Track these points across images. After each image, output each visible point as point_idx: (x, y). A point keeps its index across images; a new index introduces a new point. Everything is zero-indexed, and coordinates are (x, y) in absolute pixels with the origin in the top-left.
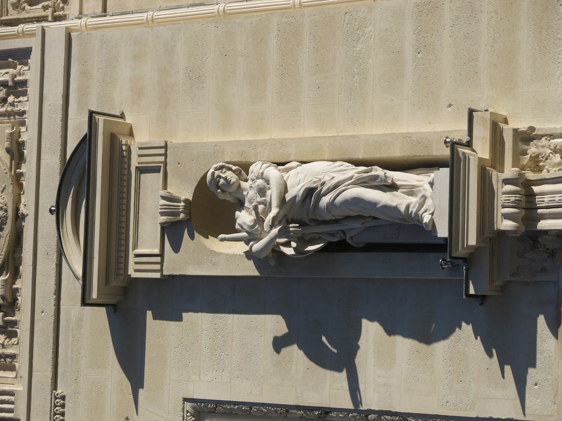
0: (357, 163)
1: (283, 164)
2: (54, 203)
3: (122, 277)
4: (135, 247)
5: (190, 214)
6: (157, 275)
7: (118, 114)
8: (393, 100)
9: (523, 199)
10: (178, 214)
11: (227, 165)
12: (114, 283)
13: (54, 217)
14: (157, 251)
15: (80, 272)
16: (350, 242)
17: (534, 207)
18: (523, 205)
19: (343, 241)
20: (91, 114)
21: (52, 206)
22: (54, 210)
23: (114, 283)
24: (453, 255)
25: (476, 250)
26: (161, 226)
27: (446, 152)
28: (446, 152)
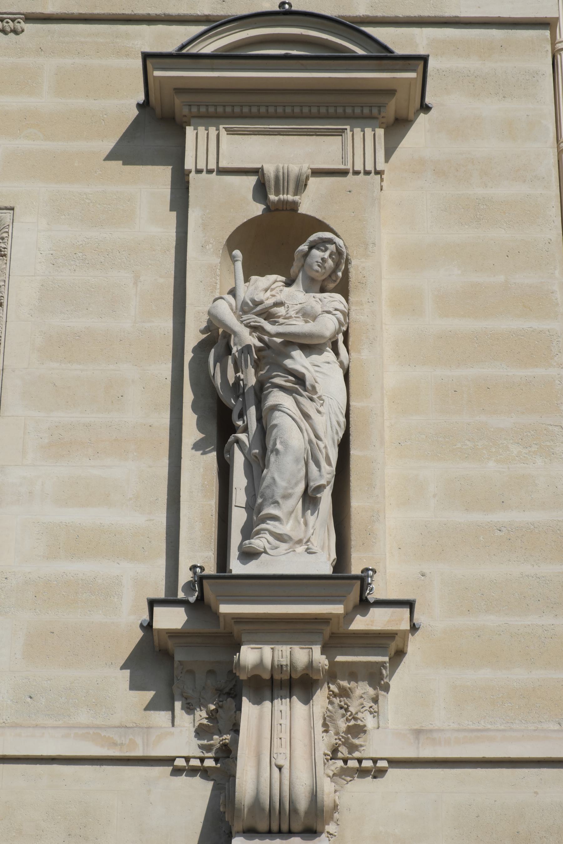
0: (344, 446)
1: (346, 343)
2: (294, 8)
3: (186, 111)
4: (230, 132)
5: (277, 210)
6: (189, 164)
7: (428, 100)
8: (434, 496)
9: (286, 677)
10: (277, 193)
11: (343, 261)
12: (178, 101)
13: (276, 8)
14: (223, 164)
15: (194, 49)
16: (232, 438)
17: (276, 692)
18: (277, 677)
19: (234, 430)
20: (424, 59)
21: (290, 5)
22: (284, 8)
23: (178, 101)
24: (205, 582)
25: (216, 615)
26: (260, 168)
27: (356, 569)
28: (356, 569)
